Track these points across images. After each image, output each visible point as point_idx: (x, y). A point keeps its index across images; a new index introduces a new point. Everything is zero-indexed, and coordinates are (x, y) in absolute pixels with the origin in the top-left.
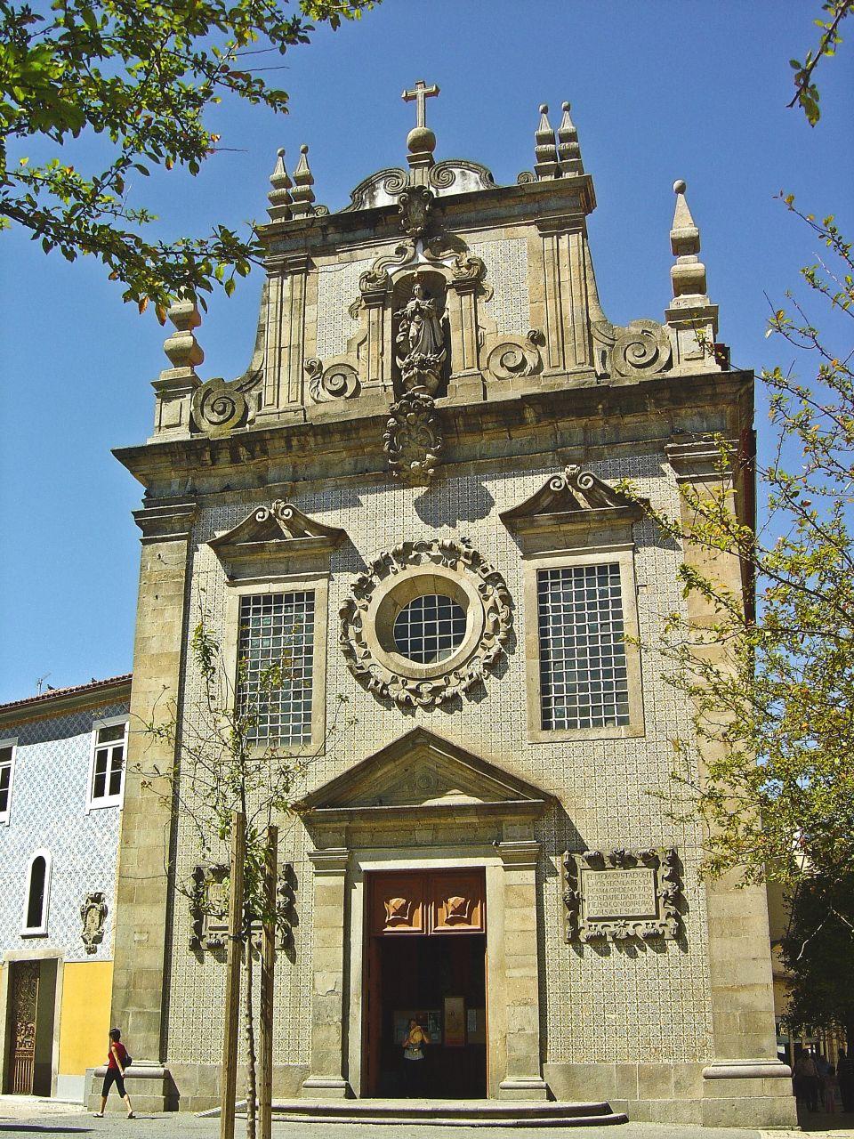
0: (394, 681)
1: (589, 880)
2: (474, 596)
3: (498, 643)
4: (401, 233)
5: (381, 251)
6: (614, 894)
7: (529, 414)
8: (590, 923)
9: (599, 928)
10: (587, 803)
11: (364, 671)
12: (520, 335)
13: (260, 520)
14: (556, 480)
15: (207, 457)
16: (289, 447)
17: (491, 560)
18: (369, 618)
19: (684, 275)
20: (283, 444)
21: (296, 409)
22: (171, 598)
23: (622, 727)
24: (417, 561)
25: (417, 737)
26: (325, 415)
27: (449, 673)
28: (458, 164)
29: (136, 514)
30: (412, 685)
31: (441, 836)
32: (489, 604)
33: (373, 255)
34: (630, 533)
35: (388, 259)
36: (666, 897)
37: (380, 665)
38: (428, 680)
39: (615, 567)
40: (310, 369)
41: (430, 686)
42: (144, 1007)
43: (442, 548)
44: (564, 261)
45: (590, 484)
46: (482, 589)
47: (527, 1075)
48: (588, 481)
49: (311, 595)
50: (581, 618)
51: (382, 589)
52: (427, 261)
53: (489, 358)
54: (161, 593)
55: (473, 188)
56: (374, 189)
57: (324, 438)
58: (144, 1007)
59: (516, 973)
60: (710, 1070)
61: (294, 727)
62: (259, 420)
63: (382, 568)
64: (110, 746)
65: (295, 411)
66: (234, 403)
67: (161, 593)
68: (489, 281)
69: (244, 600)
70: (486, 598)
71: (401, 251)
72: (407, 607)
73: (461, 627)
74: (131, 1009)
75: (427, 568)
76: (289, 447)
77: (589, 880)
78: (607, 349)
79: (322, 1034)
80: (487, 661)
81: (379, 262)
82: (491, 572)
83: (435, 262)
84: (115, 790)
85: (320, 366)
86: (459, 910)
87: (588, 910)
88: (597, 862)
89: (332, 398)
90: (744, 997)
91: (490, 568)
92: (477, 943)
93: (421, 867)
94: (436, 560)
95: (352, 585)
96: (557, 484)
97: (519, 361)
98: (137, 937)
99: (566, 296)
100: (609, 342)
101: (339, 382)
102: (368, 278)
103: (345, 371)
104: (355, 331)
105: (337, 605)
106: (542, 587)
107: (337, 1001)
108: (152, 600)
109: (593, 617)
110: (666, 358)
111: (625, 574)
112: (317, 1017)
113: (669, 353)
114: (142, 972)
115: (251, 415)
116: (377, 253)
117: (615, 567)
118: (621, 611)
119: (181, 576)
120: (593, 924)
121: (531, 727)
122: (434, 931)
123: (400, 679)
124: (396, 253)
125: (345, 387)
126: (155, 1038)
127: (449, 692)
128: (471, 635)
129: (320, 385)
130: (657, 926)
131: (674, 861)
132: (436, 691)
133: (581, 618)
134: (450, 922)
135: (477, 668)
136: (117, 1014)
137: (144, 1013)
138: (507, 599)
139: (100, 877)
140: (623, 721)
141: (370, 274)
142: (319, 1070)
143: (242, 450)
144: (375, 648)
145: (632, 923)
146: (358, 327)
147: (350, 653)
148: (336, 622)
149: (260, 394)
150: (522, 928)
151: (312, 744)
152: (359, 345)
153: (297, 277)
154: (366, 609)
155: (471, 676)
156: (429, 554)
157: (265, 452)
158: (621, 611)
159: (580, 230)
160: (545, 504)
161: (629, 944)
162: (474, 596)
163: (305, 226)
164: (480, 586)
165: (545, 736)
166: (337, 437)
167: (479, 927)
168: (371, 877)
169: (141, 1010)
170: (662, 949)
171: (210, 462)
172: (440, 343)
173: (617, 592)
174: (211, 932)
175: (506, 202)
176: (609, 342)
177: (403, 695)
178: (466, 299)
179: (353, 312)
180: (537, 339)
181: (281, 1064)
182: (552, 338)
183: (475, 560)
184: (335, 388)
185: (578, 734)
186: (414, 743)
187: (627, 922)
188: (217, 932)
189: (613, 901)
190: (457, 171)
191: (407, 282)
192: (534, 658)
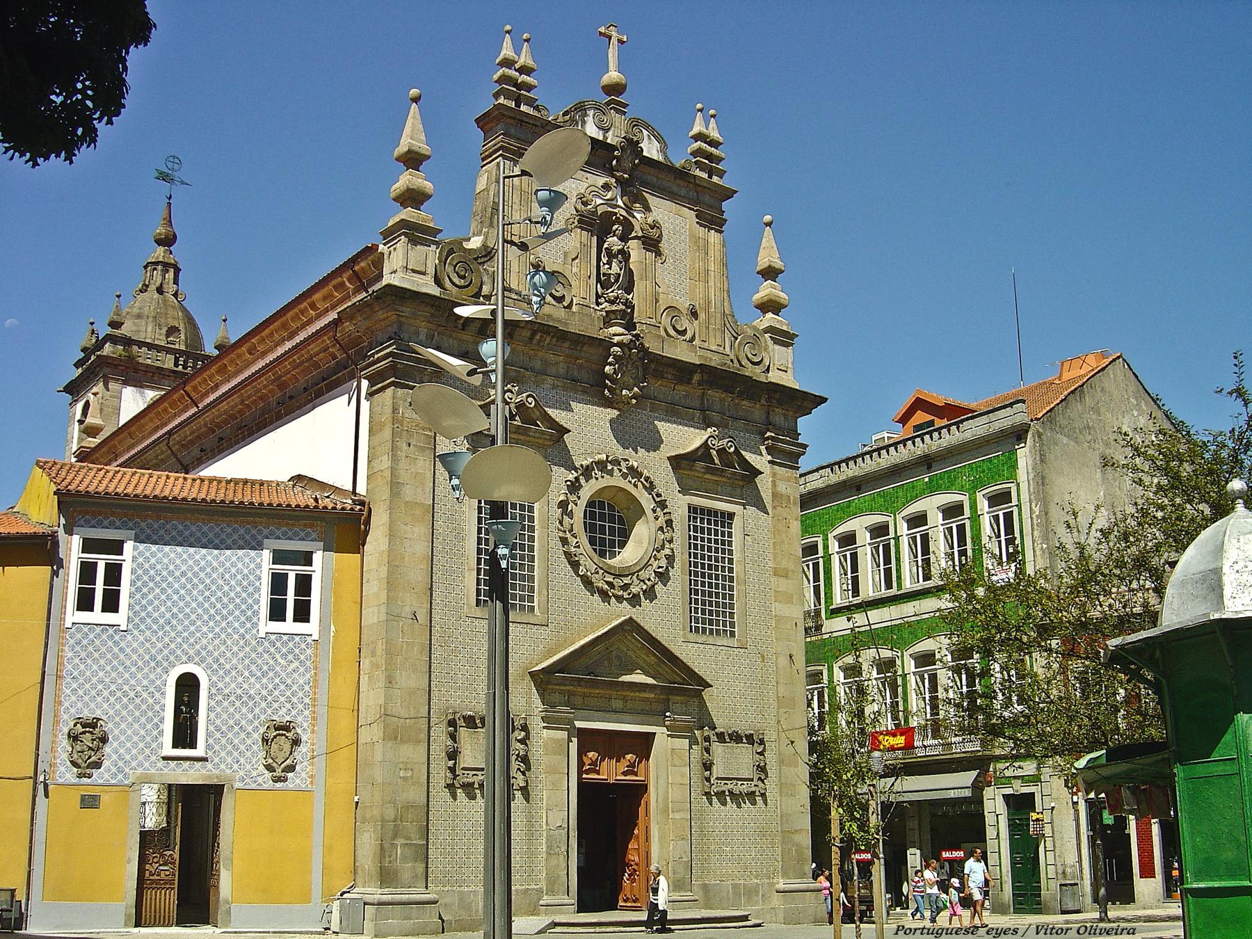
1: (717, 748)
4: (610, 171)
7: (696, 377)
12: (684, 304)
16: (531, 339)
18: (579, 511)
19: (777, 299)
20: (529, 334)
22: (422, 449)
24: (611, 473)
26: (549, 316)
27: (633, 574)
28: (647, 127)
30: (609, 578)
31: (629, 705)
33: (584, 179)
35: (597, 190)
36: (758, 766)
39: (731, 516)
42: (410, 838)
44: (711, 253)
47: (685, 891)
48: (731, 446)
51: (588, 490)
54: (413, 442)
56: (586, 115)
57: (557, 341)
58: (410, 838)
59: (678, 816)
60: (781, 886)
63: (587, 472)
64: (292, 572)
68: (664, 245)
71: (606, 187)
74: (399, 842)
75: (617, 481)
76: (531, 339)
77: (717, 748)
79: (554, 862)
80: (660, 570)
83: (629, 209)
84: (302, 614)
86: (632, 765)
87: (717, 771)
88: (721, 737)
90: (797, 838)
92: (642, 788)
94: (624, 476)
99: (711, 283)
107: (563, 835)
108: (405, 446)
111: (737, 522)
112: (549, 847)
114: (408, 807)
117: (731, 516)
126: (420, 867)
127: (635, 590)
132: (625, 587)
134: (624, 773)
135: (648, 574)
136: (386, 845)
138: (669, 523)
139: (288, 706)
142: (551, 891)
144: (584, 540)
145: (740, 783)
147: (564, 541)
150: (681, 782)
152: (573, 260)
161: (737, 798)
163: (539, 124)
166: (567, 344)
168: (582, 733)
169: (409, 842)
170: (754, 803)
173: (730, 535)
174: (464, 772)
175: (678, 181)
181: (521, 888)
182: (702, 316)
183: (650, 487)
184: (558, 294)
186: (622, 629)
190: (645, 132)
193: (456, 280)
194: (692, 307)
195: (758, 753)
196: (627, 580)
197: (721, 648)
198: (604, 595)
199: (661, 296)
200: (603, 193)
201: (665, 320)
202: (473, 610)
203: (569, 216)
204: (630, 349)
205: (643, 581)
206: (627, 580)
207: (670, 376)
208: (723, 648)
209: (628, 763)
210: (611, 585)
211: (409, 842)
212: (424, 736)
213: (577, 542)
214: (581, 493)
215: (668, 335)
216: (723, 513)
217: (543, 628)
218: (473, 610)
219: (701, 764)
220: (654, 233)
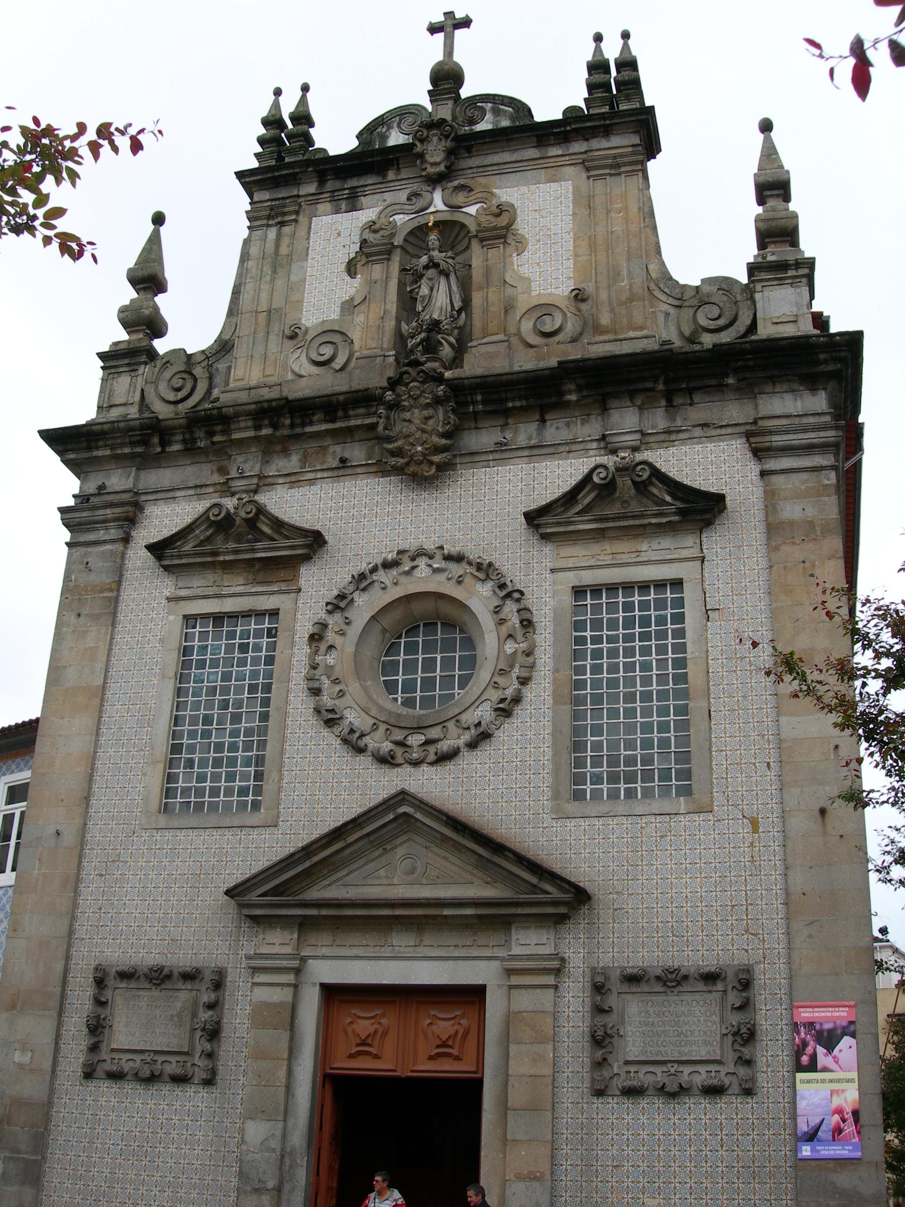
0: (375, 727)
2: (486, 620)
3: (515, 682)
5: (389, 197)
6: (662, 1029)
8: (627, 1068)
9: (641, 1075)
10: (630, 902)
11: (336, 716)
13: (212, 518)
14: (598, 470)
15: (156, 440)
17: (515, 575)
18: (347, 645)
21: (272, 383)
22: (96, 617)
23: (682, 798)
25: (401, 803)
29: (62, 510)
30: (398, 735)
32: (504, 629)
34: (698, 541)
37: (358, 709)
38: (419, 729)
40: (293, 337)
41: (423, 738)
42: (19, 1152)
43: (448, 558)
45: (646, 475)
46: (497, 610)
49: (274, 614)
50: (629, 652)
52: (446, 208)
53: (520, 321)
54: (85, 611)
55: (505, 123)
61: (240, 788)
62: (225, 398)
65: (270, 387)
66: (195, 380)
67: (85, 611)
69: (190, 620)
70: (502, 622)
72: (400, 637)
73: (470, 663)
78: (672, 311)
80: (501, 706)
81: (390, 209)
82: (510, 589)
85: (307, 331)
89: (314, 370)
91: (509, 583)
93: (397, 982)
95: (327, 604)
96: (602, 475)
97: (557, 326)
98: (18, 1057)
100: (676, 303)
101: (328, 351)
102: (371, 226)
103: (337, 338)
104: (352, 291)
105: (304, 628)
106: (579, 609)
108: (73, 619)
109: (645, 651)
110: (748, 322)
111: (690, 593)
113: (751, 317)
115: (216, 392)
116: (385, 200)
118: (685, 643)
119: (111, 590)
120: (633, 1068)
121: (556, 796)
122: (412, 1071)
123: (384, 726)
124: (408, 199)
125: (332, 359)
127: (445, 746)
128: (484, 675)
129: (304, 354)
130: (723, 1074)
131: (746, 984)
133: (629, 652)
137: (18, 1159)
138: (527, 624)
140: (686, 791)
141: (374, 223)
143: (200, 434)
144: (354, 687)
145: (687, 1070)
146: (351, 287)
148: (301, 652)
149: (229, 368)
150: (533, 1071)
151: (262, 811)
153: (287, 230)
154: (342, 633)
155: (479, 724)
156: (430, 566)
157: (226, 432)
158: (685, 643)
159: (638, 170)
160: (586, 501)
162: (486, 620)
164: (496, 607)
165: (573, 807)
167: (473, 1069)
169: (15, 1155)
171: (159, 449)
172: (458, 304)
176: (676, 303)
177: (386, 747)
178: (492, 253)
179: (351, 269)
180: (579, 296)
184: (322, 359)
185: (621, 806)
187: (681, 1069)
188: (122, 1056)
189: (662, 1039)
191: (419, 233)
192: (564, 704)
193: (171, 397)
194: (576, 292)
195: (734, 1008)
196: (434, 733)
197: (644, 820)
198: (386, 760)
199: (520, 298)
200: (410, 207)
201: (527, 326)
202: (154, 818)
203: (352, 255)
204: (407, 385)
205: (468, 728)
206: (434, 733)
207: (518, 404)
208: (652, 818)
209: (438, 1042)
210: (401, 744)
211: (15, 1155)
212: (55, 1002)
213: (341, 691)
214: (351, 614)
215: (531, 346)
216: (660, 585)
217: (268, 831)
218: (154, 818)
219: (587, 1038)
220: (503, 221)
